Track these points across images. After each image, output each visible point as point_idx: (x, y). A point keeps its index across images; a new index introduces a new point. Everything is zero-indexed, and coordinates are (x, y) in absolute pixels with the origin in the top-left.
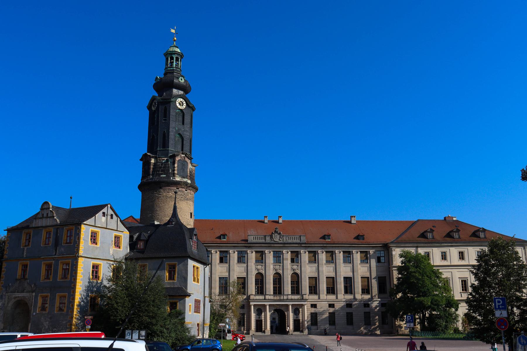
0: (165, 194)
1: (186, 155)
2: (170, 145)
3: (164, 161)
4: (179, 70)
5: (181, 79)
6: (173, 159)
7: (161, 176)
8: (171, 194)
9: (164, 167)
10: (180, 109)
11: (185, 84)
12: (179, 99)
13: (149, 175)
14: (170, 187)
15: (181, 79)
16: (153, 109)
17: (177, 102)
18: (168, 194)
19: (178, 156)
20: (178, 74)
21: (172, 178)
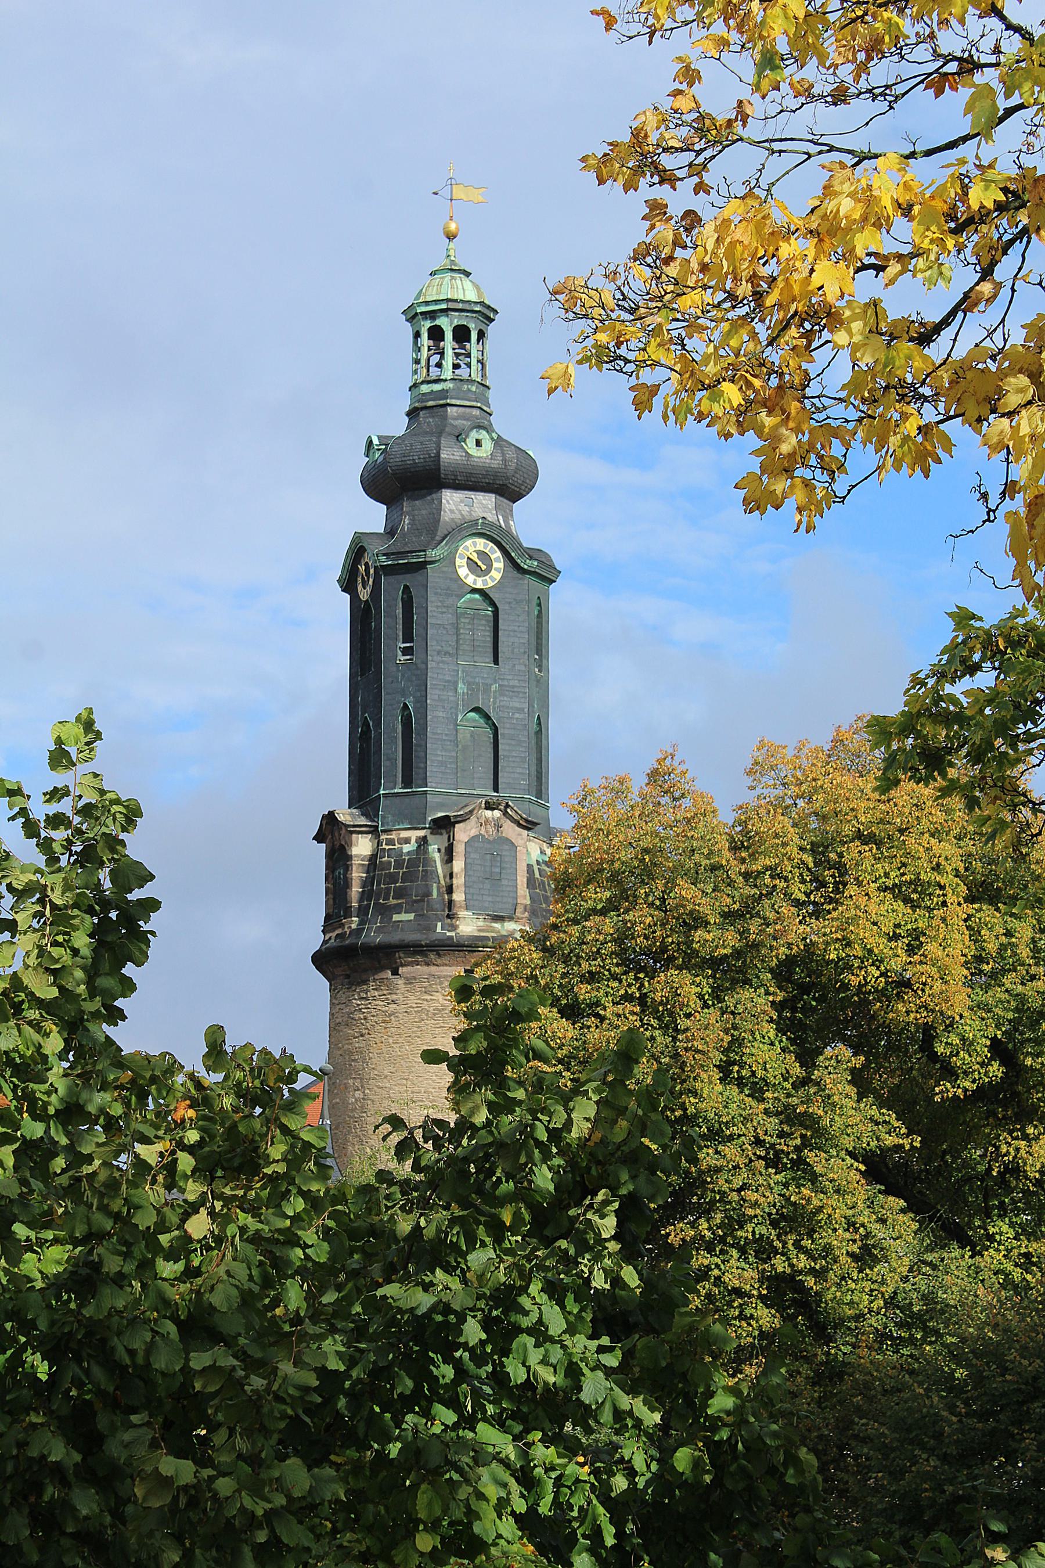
0: (412, 1000)
1: (505, 813)
2: (432, 768)
3: (406, 848)
4: (474, 389)
5: (478, 443)
6: (446, 836)
7: (396, 917)
8: (441, 998)
9: (407, 877)
10: (474, 591)
11: (497, 463)
12: (469, 543)
13: (348, 914)
14: (433, 969)
15: (478, 443)
16: (364, 594)
17: (458, 562)
18: (429, 997)
19: (462, 819)
20: (468, 410)
21: (439, 924)
